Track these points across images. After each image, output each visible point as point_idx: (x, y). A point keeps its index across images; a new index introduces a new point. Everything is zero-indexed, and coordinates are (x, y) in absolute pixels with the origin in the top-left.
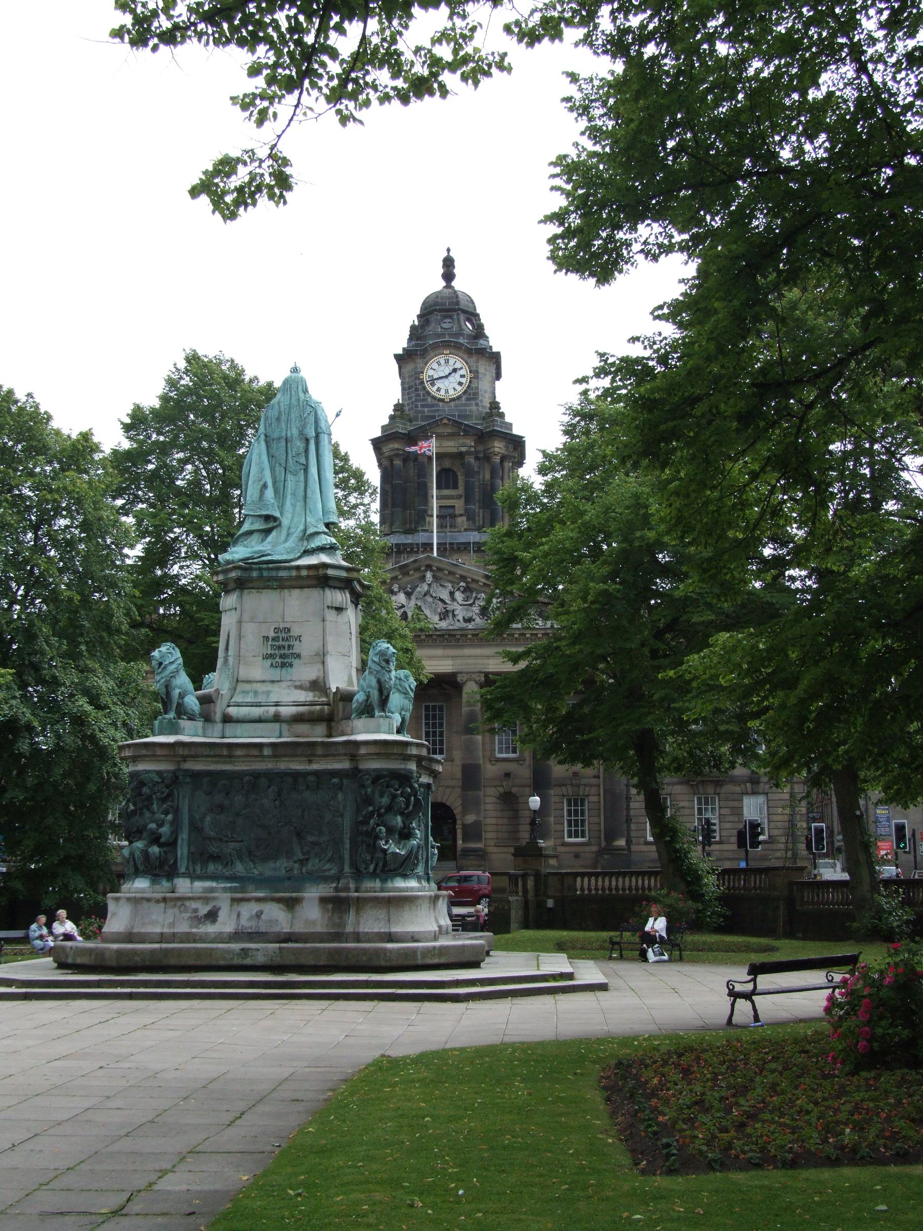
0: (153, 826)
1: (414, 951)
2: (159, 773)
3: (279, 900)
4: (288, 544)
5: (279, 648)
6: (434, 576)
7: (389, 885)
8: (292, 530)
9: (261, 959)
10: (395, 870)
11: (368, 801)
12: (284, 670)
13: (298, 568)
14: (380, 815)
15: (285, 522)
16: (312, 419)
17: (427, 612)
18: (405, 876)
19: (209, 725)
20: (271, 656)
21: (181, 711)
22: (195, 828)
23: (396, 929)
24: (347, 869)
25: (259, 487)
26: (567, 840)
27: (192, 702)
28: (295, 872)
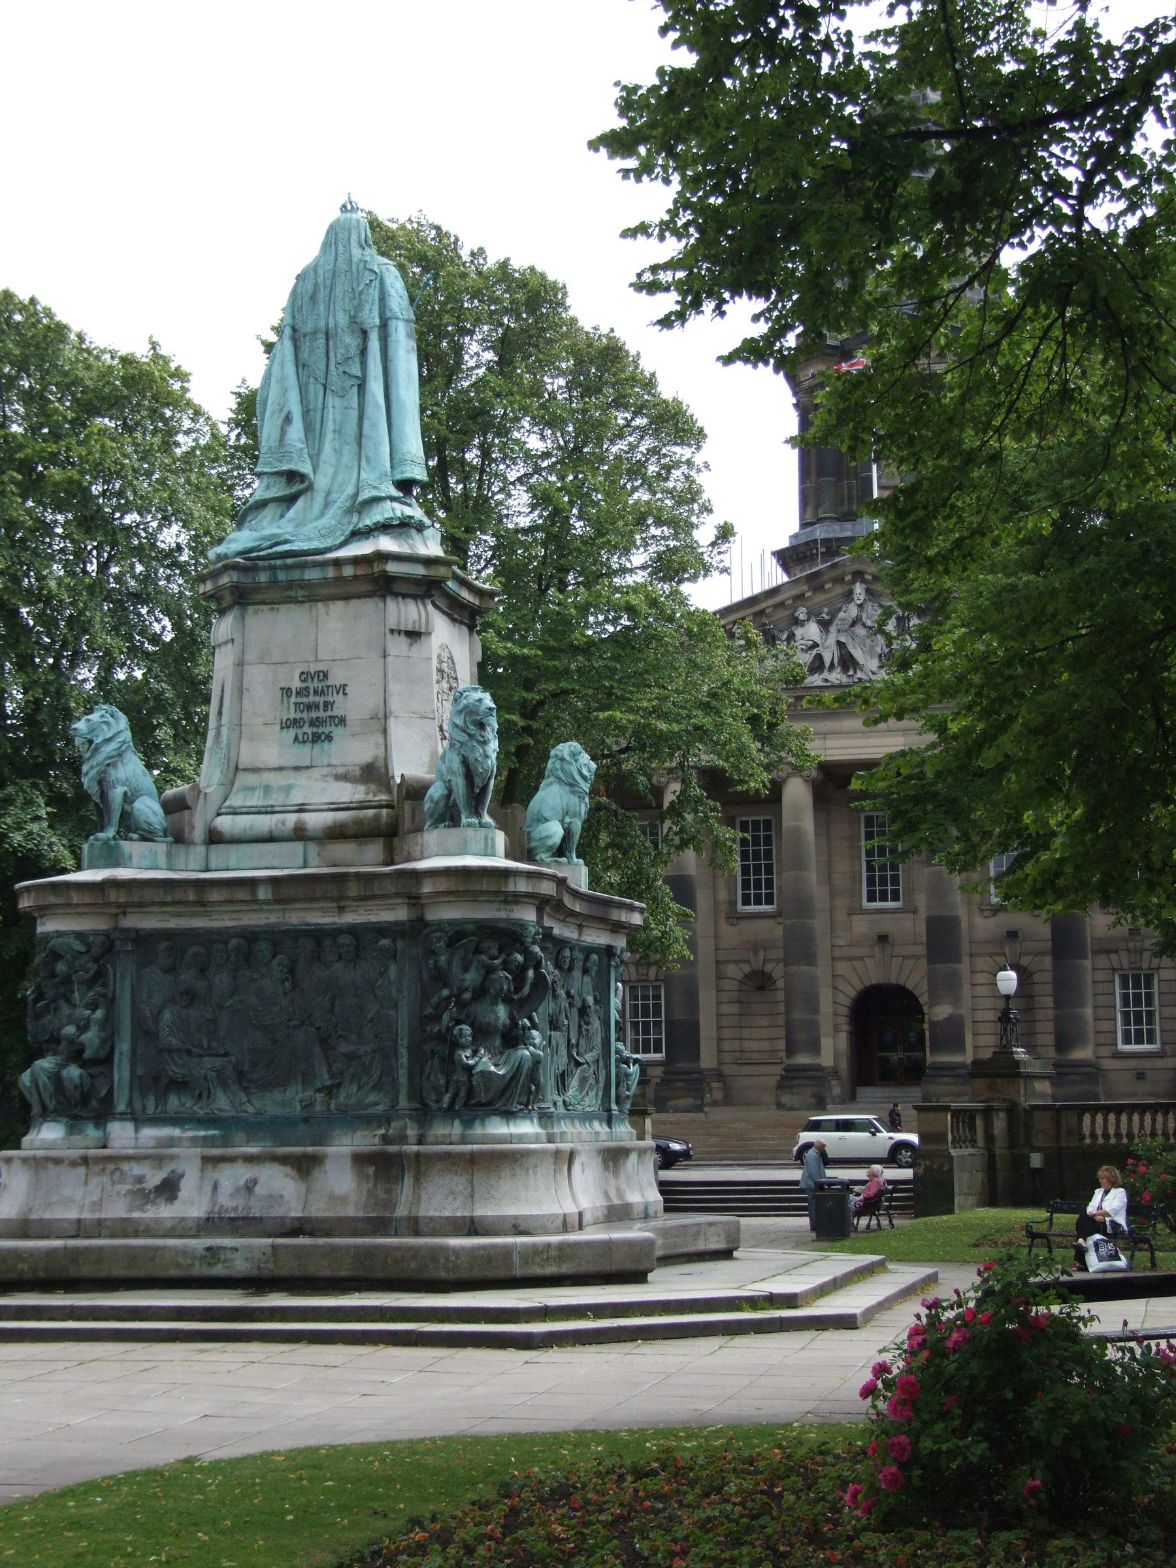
0: (71, 1030)
1: (507, 1251)
2: (80, 936)
3: (284, 1160)
4: (324, 521)
5: (309, 707)
6: (868, 591)
7: (478, 1130)
8: (334, 496)
9: (240, 1267)
10: (490, 1103)
11: (441, 977)
12: (317, 747)
13: (337, 563)
14: (462, 1005)
15: (321, 482)
16: (374, 293)
17: (858, 654)
18: (508, 1115)
19: (181, 847)
20: (296, 723)
21: (129, 825)
22: (144, 1032)
23: (485, 1211)
24: (403, 1102)
25: (280, 422)
26: (1122, 1047)
27: (149, 809)
28: (318, 1108)
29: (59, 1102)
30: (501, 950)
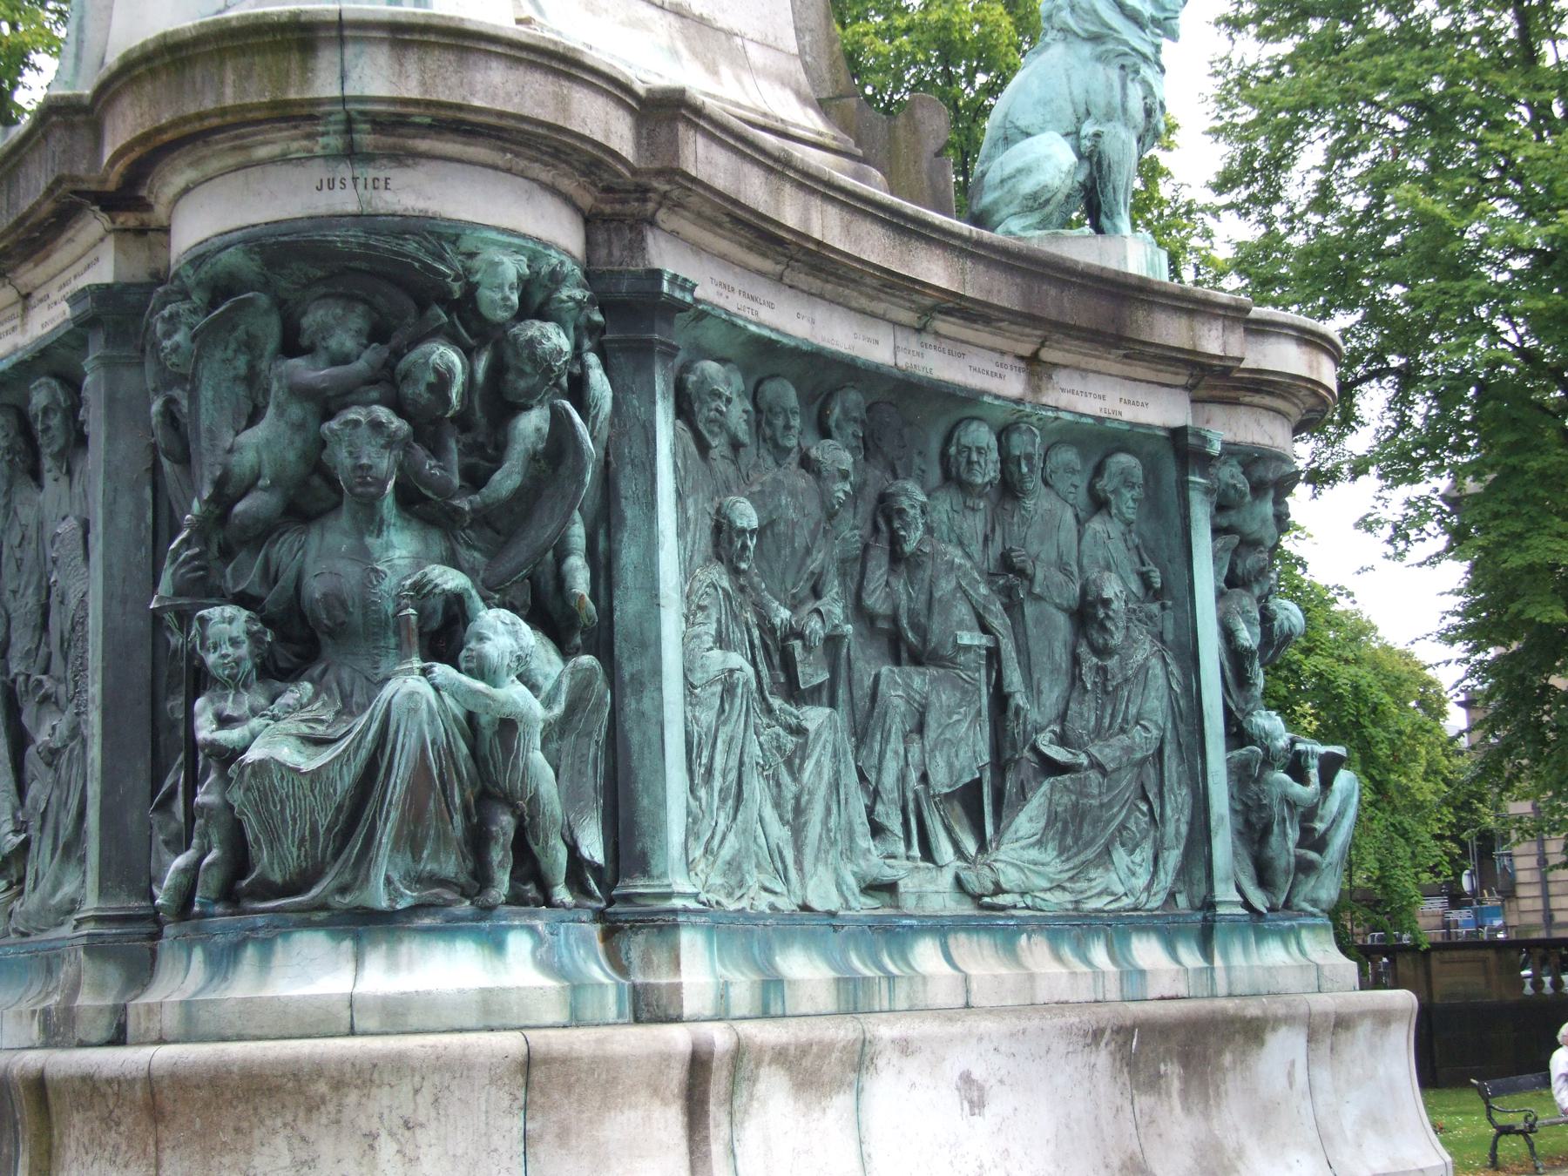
30: (377, 334)
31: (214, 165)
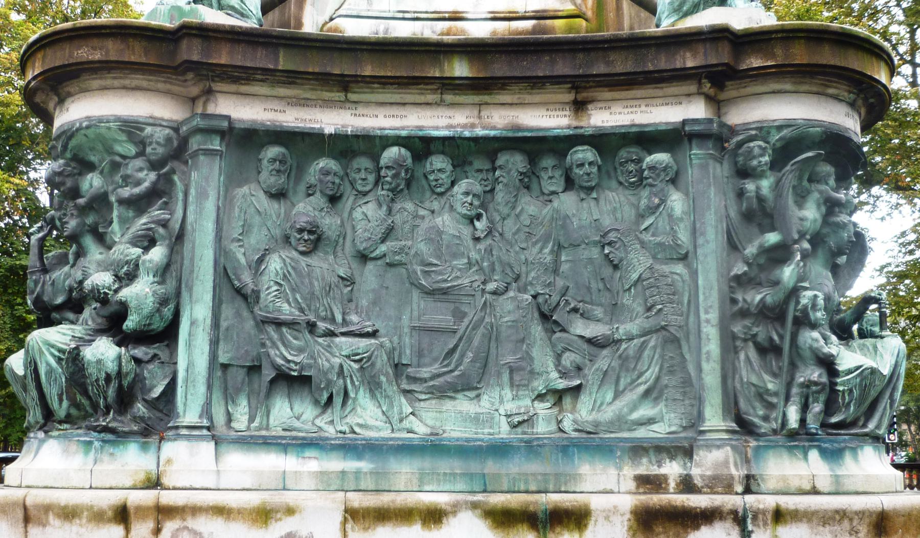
0: (102, 279)
2: (131, 128)
10: (853, 424)
22: (233, 290)
24: (715, 419)
29: (74, 404)
31: (805, 88)
